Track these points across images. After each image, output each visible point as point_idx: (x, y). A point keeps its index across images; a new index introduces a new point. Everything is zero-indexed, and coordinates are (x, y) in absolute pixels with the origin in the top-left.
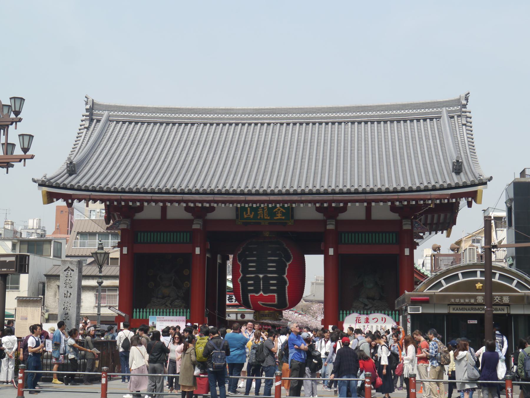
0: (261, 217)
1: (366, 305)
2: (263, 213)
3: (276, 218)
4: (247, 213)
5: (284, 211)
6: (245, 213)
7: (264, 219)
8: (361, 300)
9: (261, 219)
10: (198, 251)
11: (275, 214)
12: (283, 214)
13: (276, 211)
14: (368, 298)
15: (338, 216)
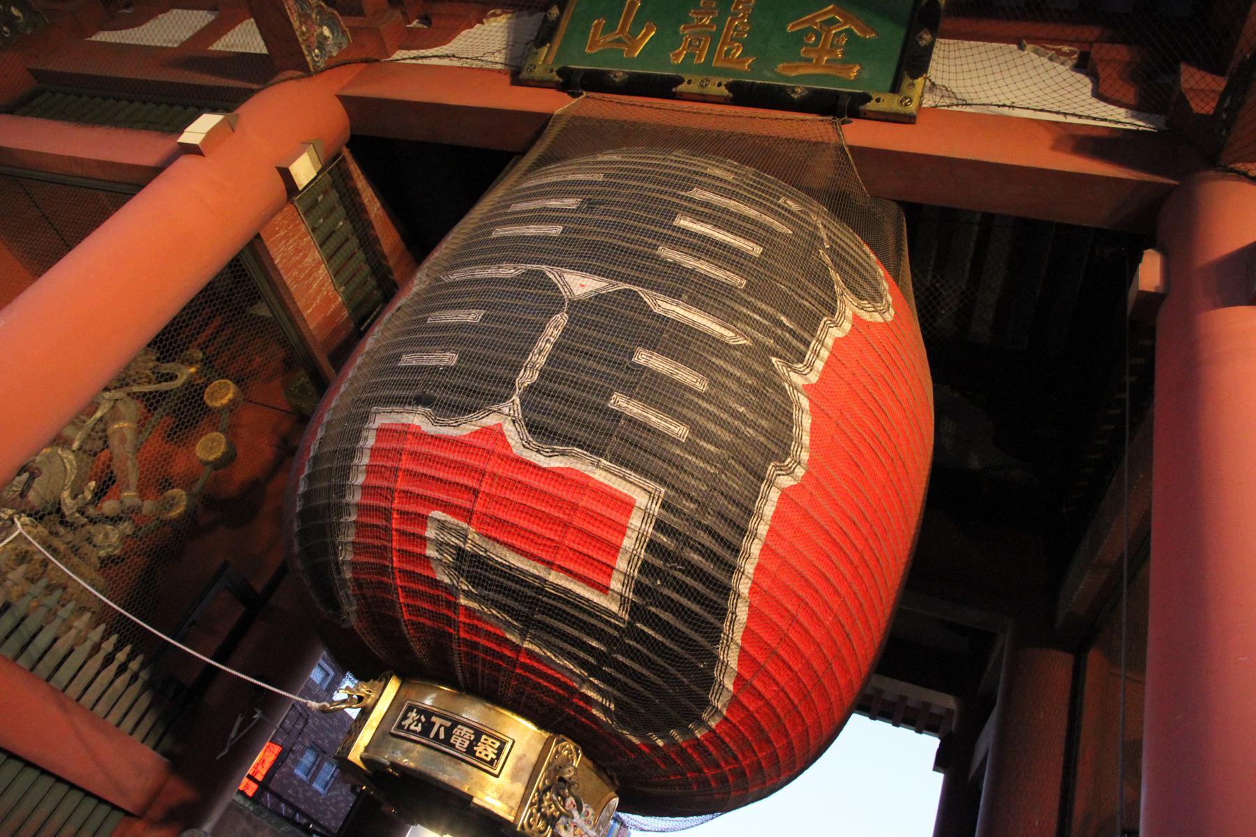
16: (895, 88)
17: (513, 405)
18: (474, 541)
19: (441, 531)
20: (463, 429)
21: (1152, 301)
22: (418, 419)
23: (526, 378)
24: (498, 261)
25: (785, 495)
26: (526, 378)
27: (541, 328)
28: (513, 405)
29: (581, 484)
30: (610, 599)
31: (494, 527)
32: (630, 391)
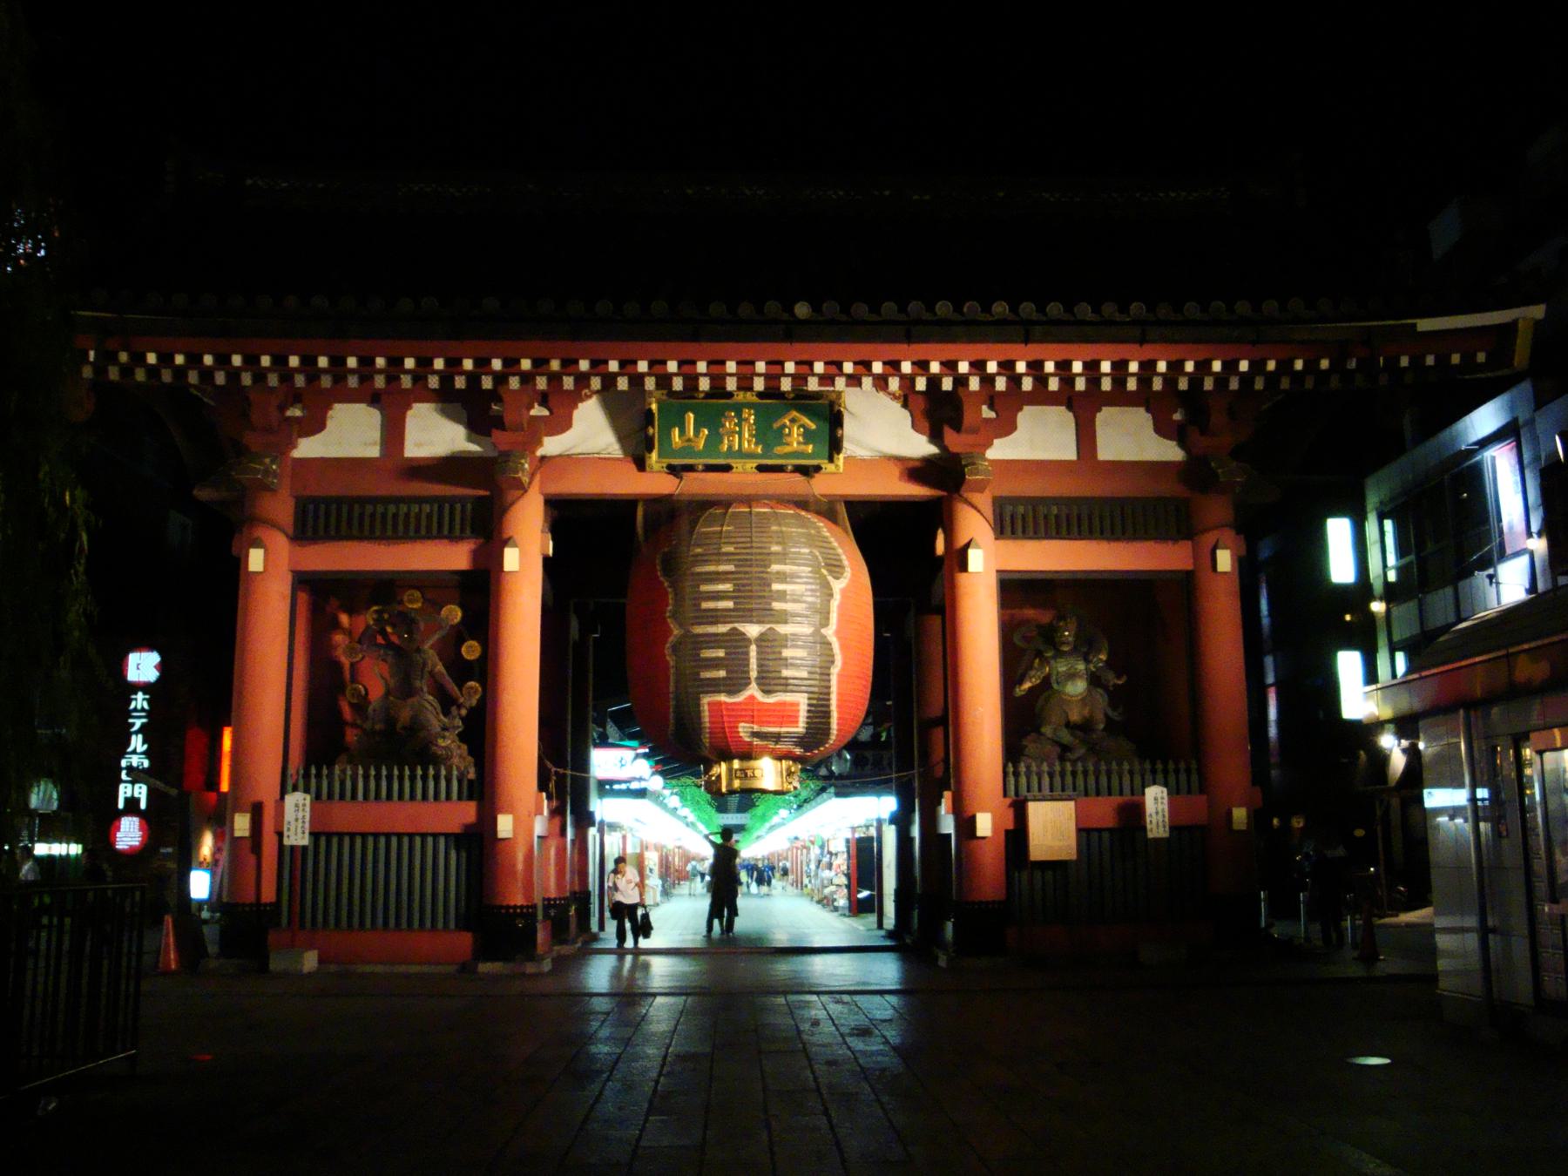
0: (730, 447)
1: (1065, 748)
2: (740, 434)
3: (779, 450)
4: (682, 432)
5: (813, 427)
6: (677, 431)
7: (742, 455)
8: (1047, 730)
9: (730, 453)
10: (511, 559)
11: (780, 436)
12: (808, 436)
13: (784, 426)
14: (1068, 725)
15: (990, 444)
16: (831, 460)
17: (754, 685)
18: (756, 728)
19: (744, 730)
20: (740, 698)
21: (941, 558)
22: (723, 698)
23: (754, 674)
24: (715, 623)
25: (840, 676)
26: (754, 674)
27: (747, 653)
28: (754, 685)
29: (784, 704)
30: (800, 727)
31: (761, 723)
32: (786, 666)
